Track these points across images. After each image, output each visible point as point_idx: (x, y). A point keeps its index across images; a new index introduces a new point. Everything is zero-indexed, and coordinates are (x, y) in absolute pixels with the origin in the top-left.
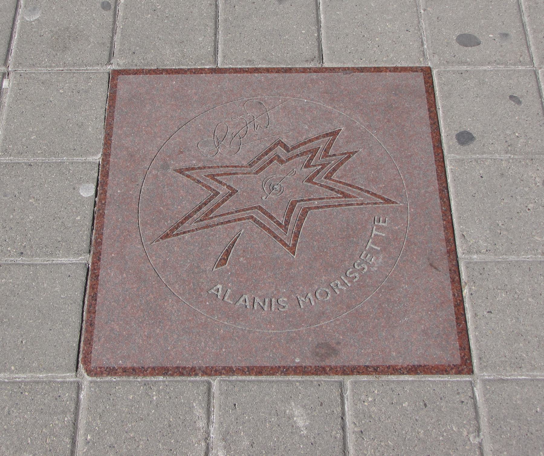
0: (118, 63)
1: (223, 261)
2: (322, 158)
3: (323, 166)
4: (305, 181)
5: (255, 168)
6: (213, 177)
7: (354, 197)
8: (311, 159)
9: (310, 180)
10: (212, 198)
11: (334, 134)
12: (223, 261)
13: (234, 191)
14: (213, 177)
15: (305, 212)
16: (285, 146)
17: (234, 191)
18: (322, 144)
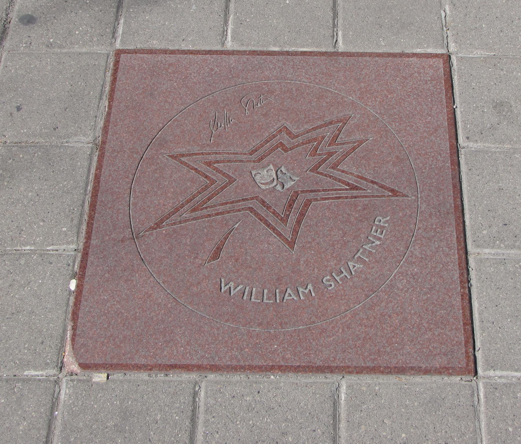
0: (118, 45)
1: (216, 255)
2: (328, 146)
3: (330, 154)
4: (310, 171)
5: (254, 157)
6: (209, 164)
7: (365, 190)
8: (316, 149)
9: (315, 169)
10: (207, 187)
11: (345, 121)
12: (216, 255)
13: (231, 181)
14: (209, 164)
15: (307, 204)
16: (289, 133)
17: (231, 181)
18: (328, 133)
